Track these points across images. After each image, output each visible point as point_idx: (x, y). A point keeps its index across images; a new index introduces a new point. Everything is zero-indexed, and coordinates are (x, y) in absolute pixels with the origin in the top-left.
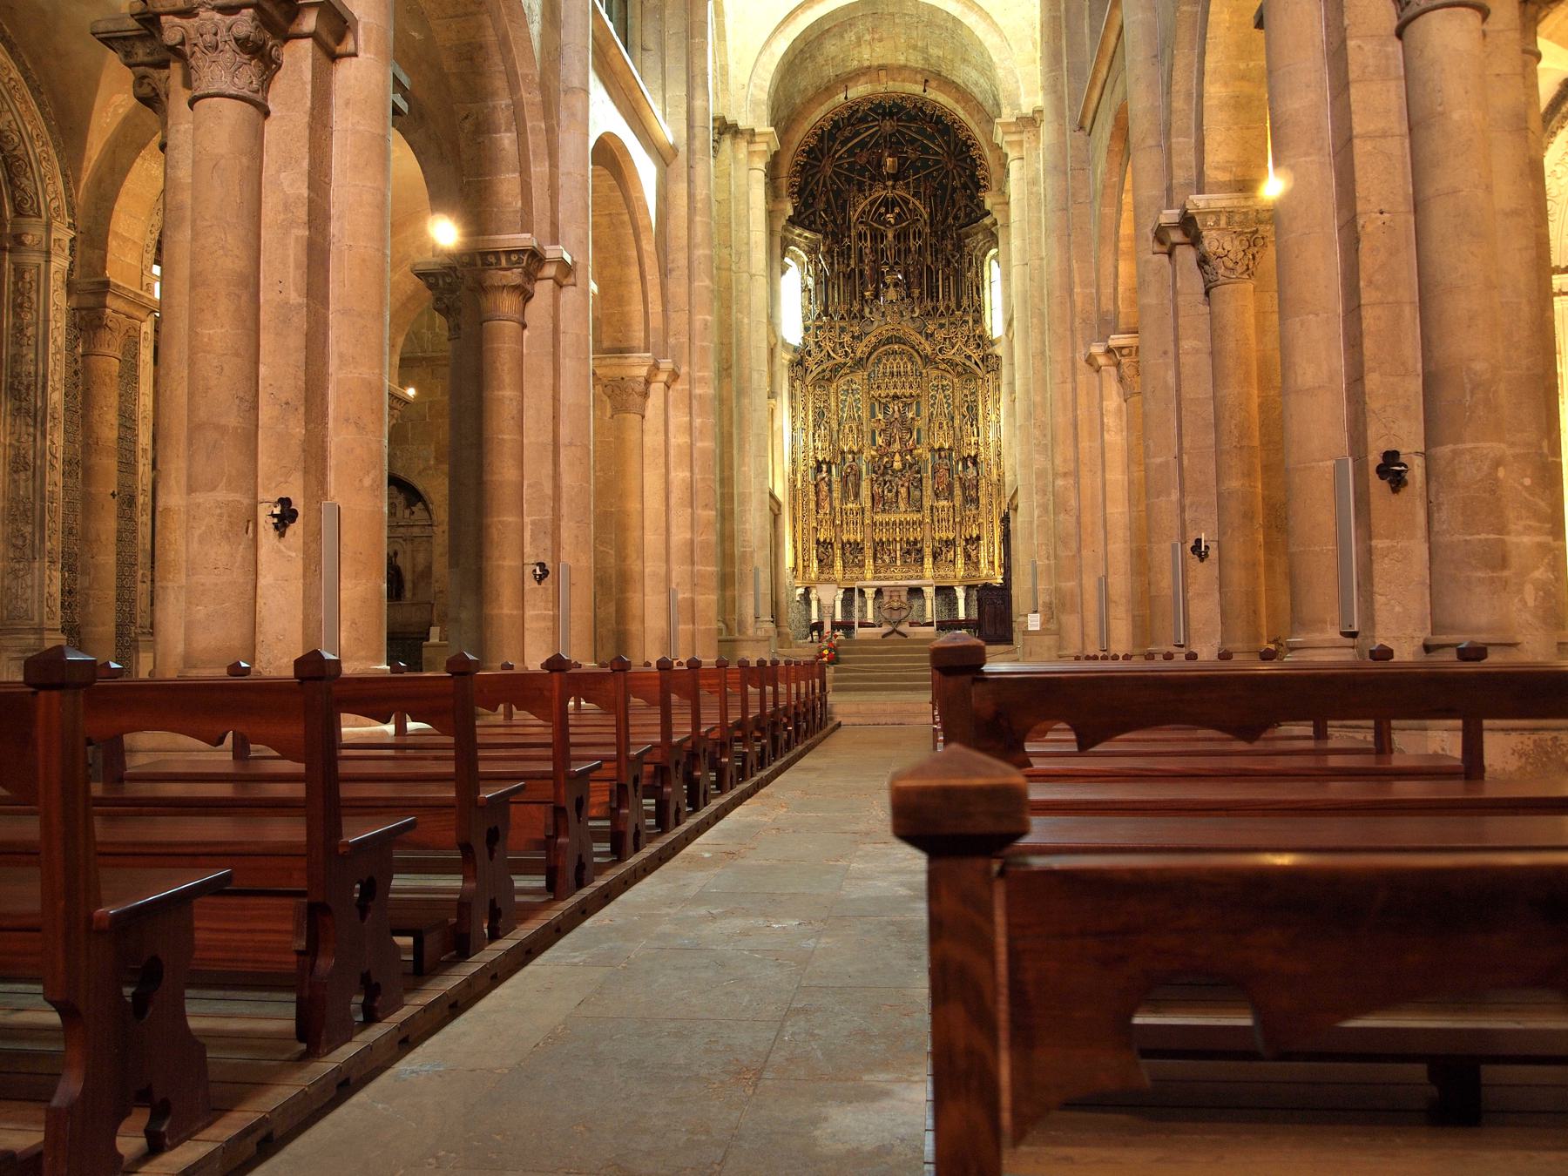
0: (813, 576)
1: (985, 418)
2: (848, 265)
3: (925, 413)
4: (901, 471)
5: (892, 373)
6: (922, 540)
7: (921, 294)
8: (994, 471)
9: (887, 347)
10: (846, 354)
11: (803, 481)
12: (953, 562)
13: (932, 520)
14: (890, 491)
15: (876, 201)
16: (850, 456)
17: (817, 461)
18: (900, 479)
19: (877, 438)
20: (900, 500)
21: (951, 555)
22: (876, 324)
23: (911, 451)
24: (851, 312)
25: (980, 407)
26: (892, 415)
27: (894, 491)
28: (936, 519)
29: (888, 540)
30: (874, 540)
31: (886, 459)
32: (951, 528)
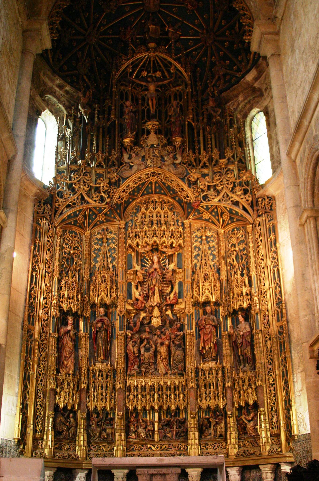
0: (46, 451)
1: (257, 265)
2: (108, 120)
3: (188, 264)
4: (160, 328)
6: (186, 409)
7: (183, 142)
8: (274, 323)
9: (147, 196)
10: (102, 200)
11: (42, 331)
12: (224, 437)
14: (147, 350)
16: (102, 310)
18: (160, 337)
19: (134, 290)
20: (159, 360)
22: (135, 168)
23: (172, 306)
24: (109, 160)
25: (252, 254)
26: (151, 267)
27: (152, 350)
28: (201, 383)
29: (144, 409)
30: (127, 409)
31: (143, 315)
32: (221, 395)
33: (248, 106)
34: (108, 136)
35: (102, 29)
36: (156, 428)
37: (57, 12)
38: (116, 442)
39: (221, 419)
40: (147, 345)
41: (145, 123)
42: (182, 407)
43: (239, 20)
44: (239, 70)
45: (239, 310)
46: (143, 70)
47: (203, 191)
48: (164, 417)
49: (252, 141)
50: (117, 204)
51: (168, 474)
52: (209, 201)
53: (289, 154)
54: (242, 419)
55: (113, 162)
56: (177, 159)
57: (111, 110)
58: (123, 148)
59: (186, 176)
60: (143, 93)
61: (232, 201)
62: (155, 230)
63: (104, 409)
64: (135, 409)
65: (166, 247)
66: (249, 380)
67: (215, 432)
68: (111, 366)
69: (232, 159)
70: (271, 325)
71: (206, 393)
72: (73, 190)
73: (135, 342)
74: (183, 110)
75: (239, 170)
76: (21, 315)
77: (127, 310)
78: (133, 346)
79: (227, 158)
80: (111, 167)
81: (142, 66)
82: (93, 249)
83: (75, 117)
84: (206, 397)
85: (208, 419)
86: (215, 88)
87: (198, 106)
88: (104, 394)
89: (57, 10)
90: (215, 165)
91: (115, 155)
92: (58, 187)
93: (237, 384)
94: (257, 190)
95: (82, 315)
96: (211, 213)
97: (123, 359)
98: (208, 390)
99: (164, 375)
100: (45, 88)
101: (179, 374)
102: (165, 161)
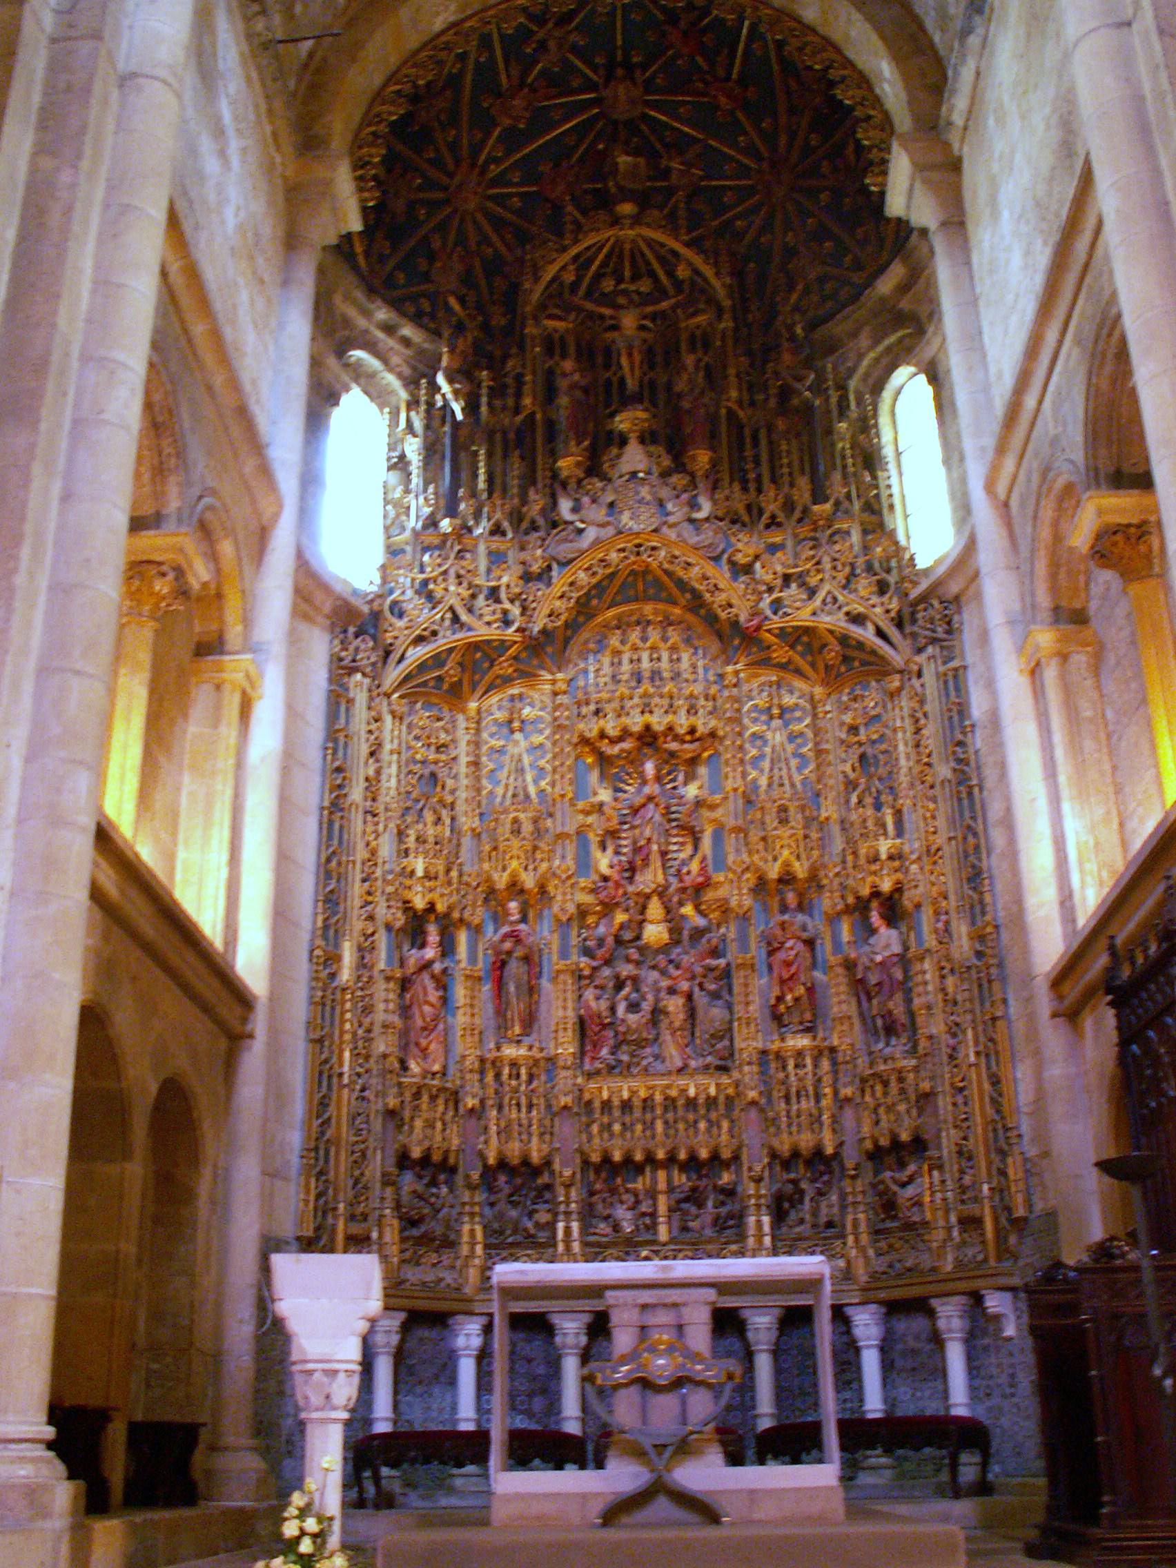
2: (517, 410)
4: (664, 949)
5: (638, 677)
6: (736, 1158)
7: (714, 464)
11: (362, 964)
13: (770, 1101)
14: (633, 1007)
15: (591, 261)
17: (407, 907)
21: (829, 1206)
22: (591, 534)
27: (646, 1006)
30: (586, 1163)
33: (884, 361)
34: (517, 453)
35: (494, 170)
36: (662, 1208)
37: (374, 134)
38: (561, 1247)
39: (828, 1183)
40: (634, 995)
41: (612, 415)
42: (726, 1154)
43: (855, 132)
44: (858, 266)
45: (869, 901)
46: (604, 275)
47: (770, 590)
48: (680, 1179)
49: (898, 454)
50: (544, 632)
51: (685, 1305)
52: (786, 614)
53: (990, 487)
54: (882, 1182)
55: (533, 522)
56: (699, 509)
57: (524, 384)
58: (557, 484)
59: (723, 552)
60: (610, 335)
61: (847, 614)
62: (645, 695)
63: (526, 1162)
64: (607, 1159)
65: (677, 738)
66: (901, 1080)
67: (815, 1213)
68: (542, 1050)
69: (846, 504)
70: (955, 936)
71: (788, 1117)
72: (430, 596)
73: (602, 987)
74: (713, 377)
75: (865, 532)
76: (306, 924)
77: (579, 906)
78: (598, 998)
79: (832, 502)
80: (527, 533)
81: (604, 265)
82: (485, 748)
83: (430, 404)
84: (789, 1125)
85: (795, 1182)
86: (797, 317)
87: (752, 365)
88: (525, 1122)
89: (373, 129)
90: (800, 520)
91: (536, 503)
92: (391, 592)
93: (868, 1090)
94: (911, 582)
95: (461, 920)
96: (792, 647)
97: (570, 1033)
98: (795, 1107)
99: (680, 1071)
100: (347, 333)
101: (718, 1068)
102: (668, 514)
